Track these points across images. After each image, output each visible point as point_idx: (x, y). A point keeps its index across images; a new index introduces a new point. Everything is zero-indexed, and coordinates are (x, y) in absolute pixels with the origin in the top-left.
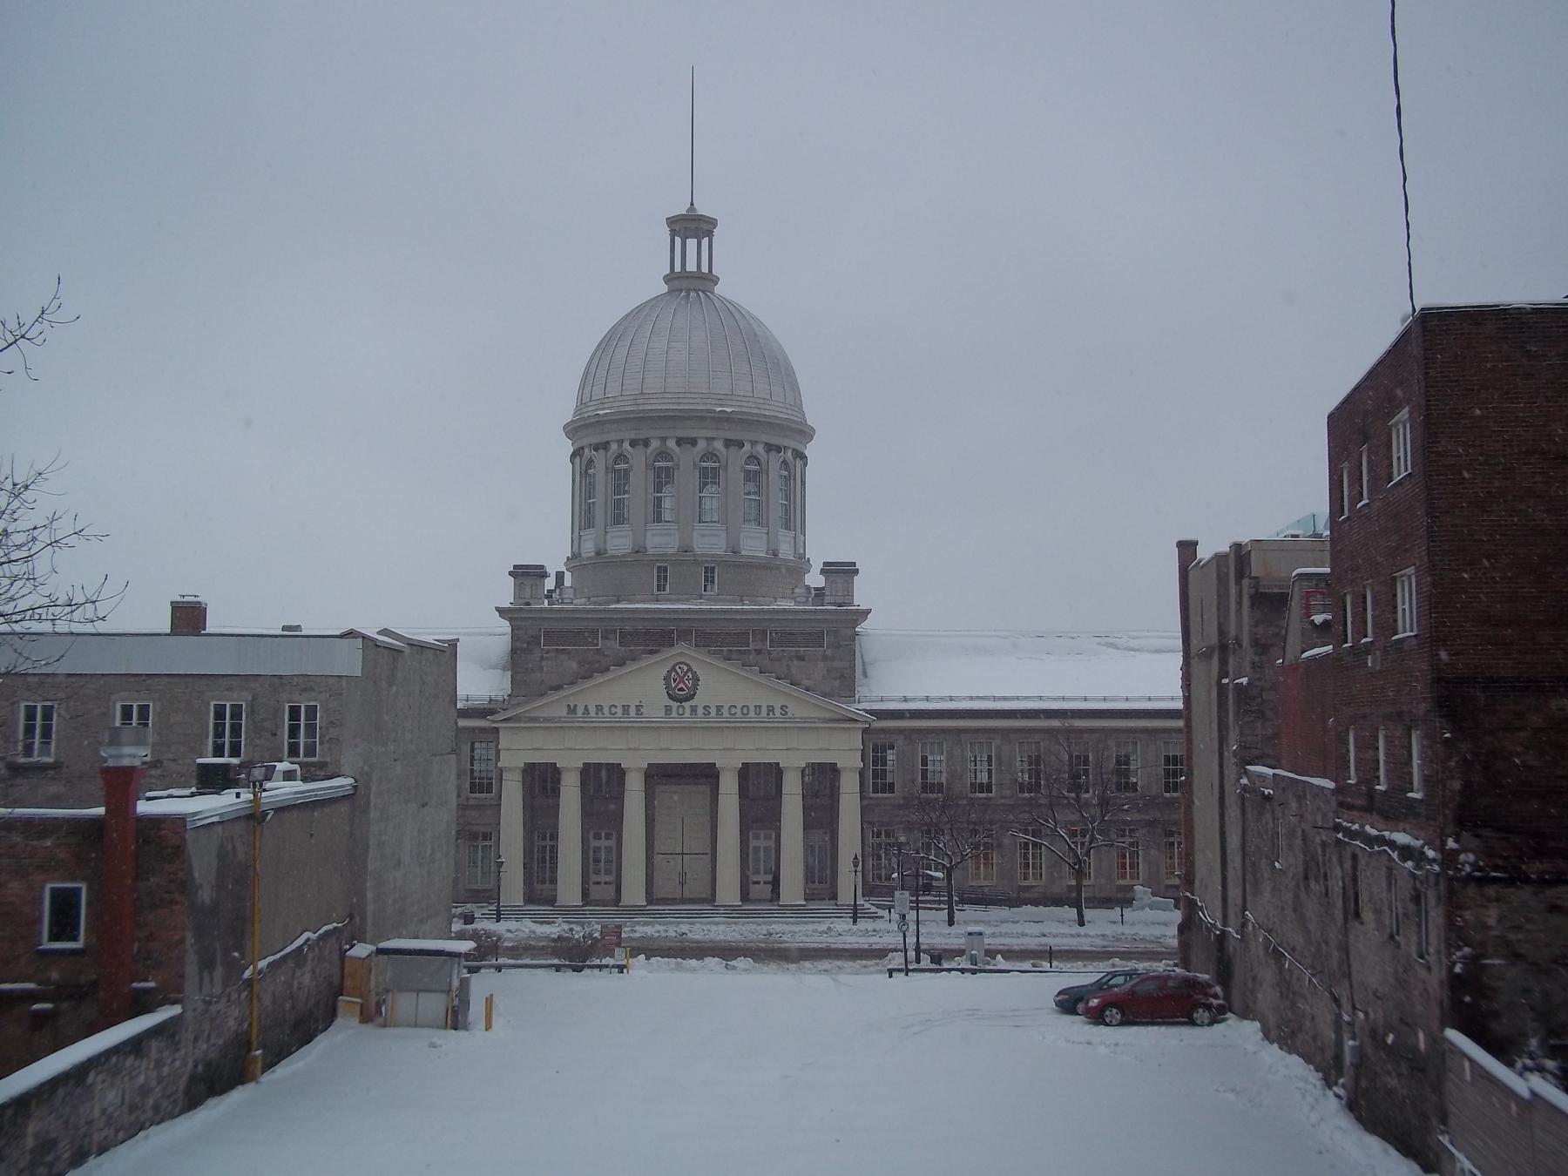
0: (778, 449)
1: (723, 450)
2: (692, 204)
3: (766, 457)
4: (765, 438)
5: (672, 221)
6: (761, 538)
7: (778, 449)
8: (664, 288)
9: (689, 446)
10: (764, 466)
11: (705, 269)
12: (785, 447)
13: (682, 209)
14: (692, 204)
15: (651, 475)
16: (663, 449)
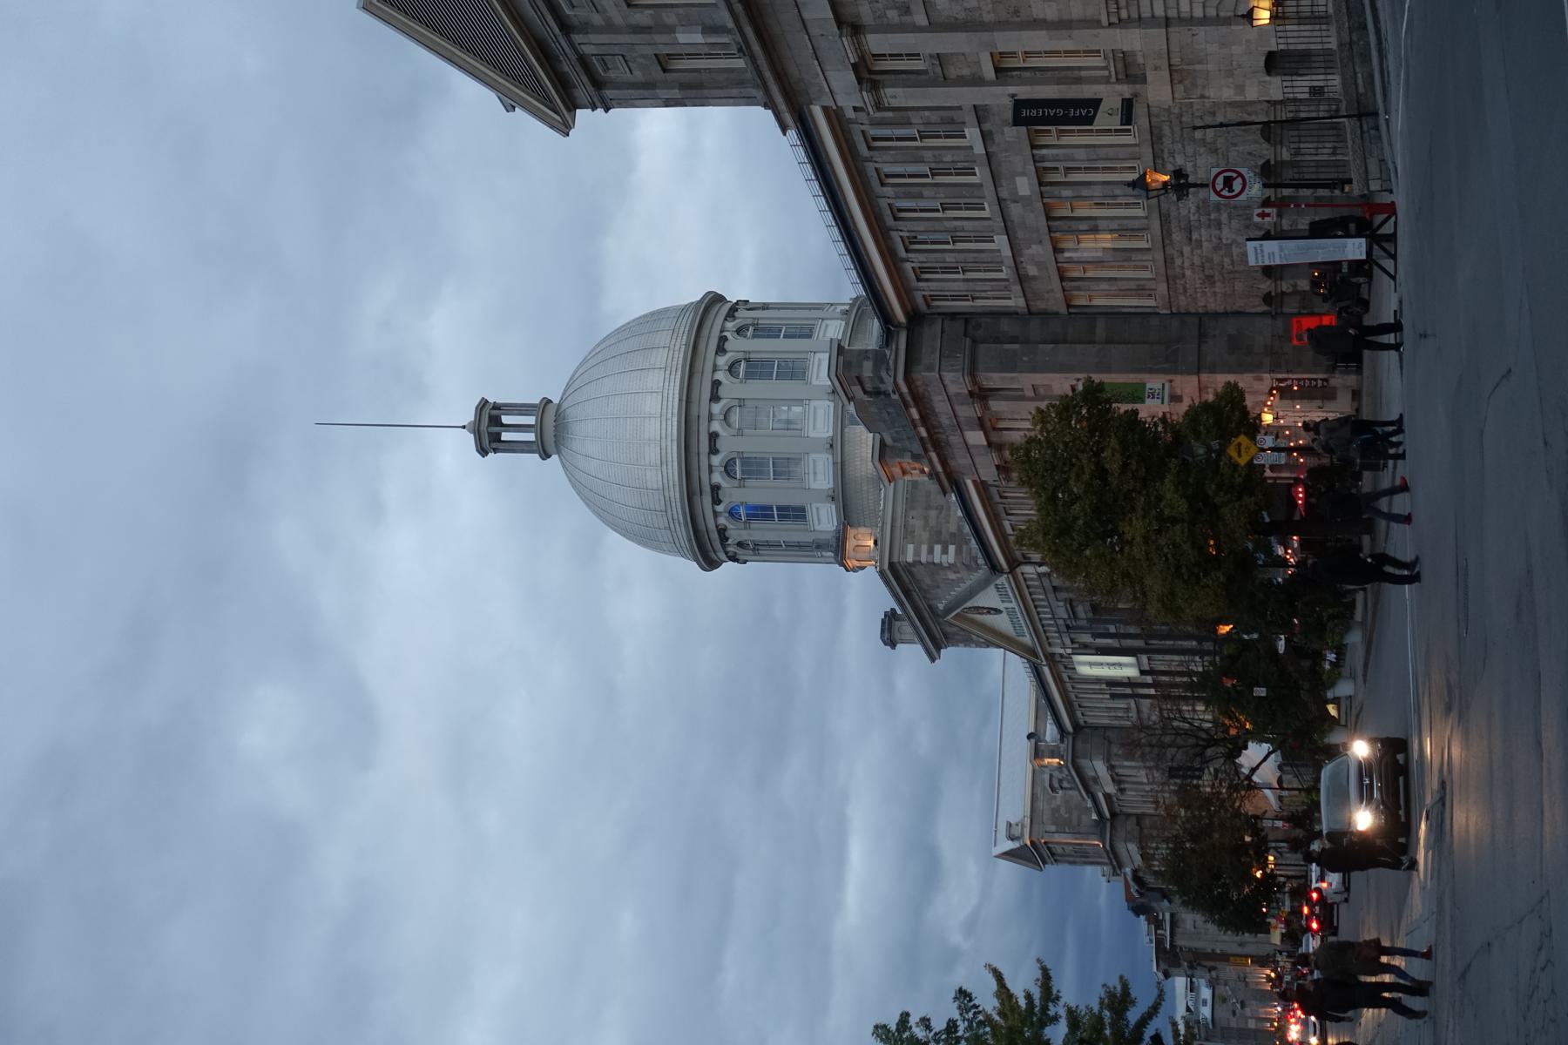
0: (723, 339)
1: (729, 355)
2: (464, 427)
3: (740, 320)
4: (704, 458)
5: (483, 451)
6: (827, 326)
7: (723, 339)
8: (555, 457)
9: (720, 492)
10: (741, 356)
11: (531, 420)
12: (722, 331)
13: (469, 439)
14: (464, 427)
15: (749, 483)
16: (723, 469)
